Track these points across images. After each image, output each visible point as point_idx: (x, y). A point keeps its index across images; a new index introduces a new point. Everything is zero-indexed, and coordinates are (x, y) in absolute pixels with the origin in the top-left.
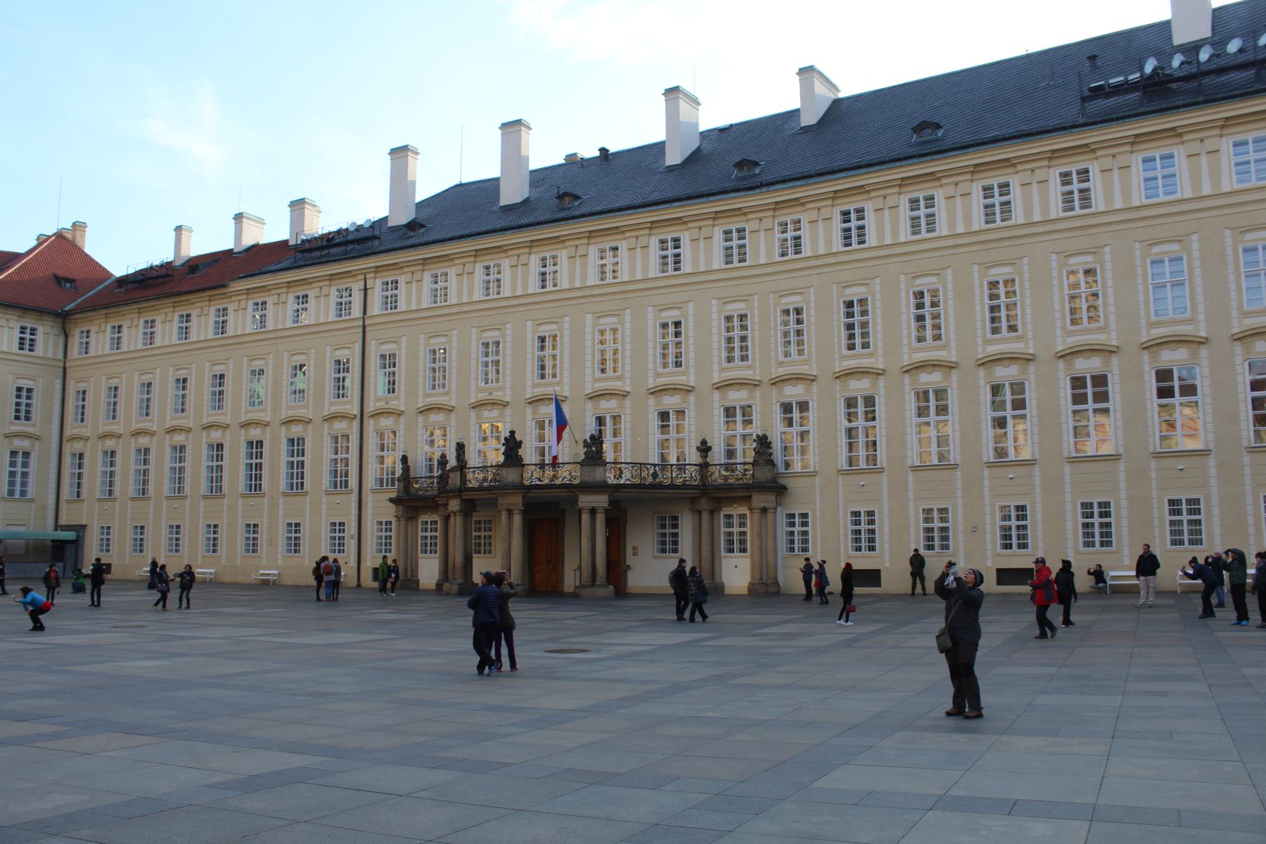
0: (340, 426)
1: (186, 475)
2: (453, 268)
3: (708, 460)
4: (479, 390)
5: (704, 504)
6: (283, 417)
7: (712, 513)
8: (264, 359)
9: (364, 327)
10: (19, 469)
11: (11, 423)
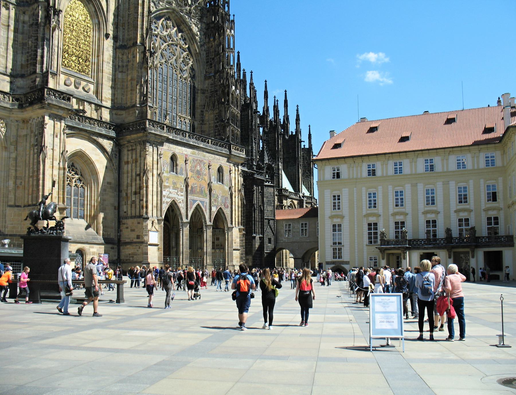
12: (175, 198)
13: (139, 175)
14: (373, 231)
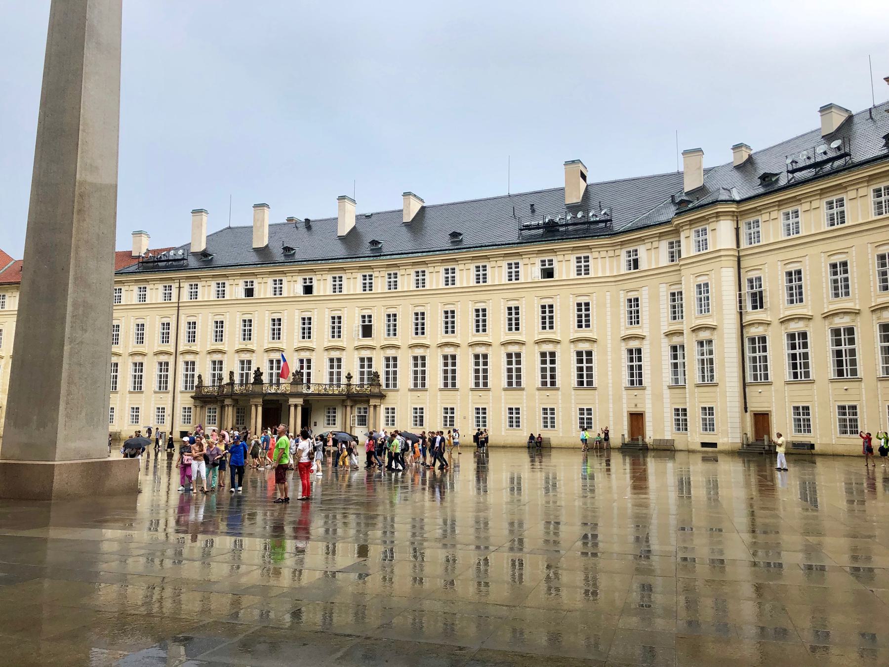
0: (164, 358)
3: (351, 382)
4: (240, 344)
5: (349, 403)
7: (352, 407)
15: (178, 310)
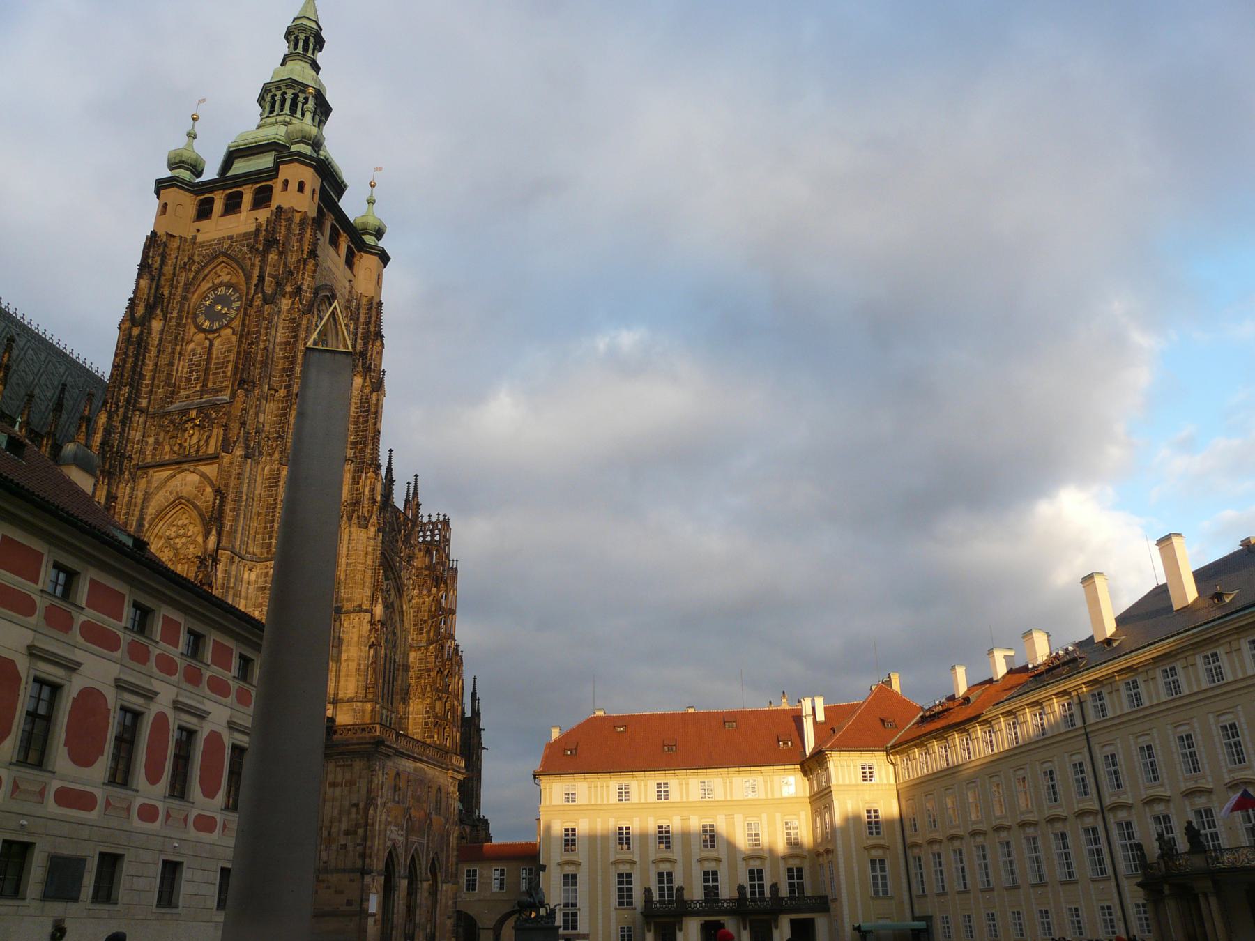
0: (1089, 821)
1: (1072, 860)
2: (1178, 663)
4: (1186, 780)
6: (1047, 816)
8: (1080, 753)
9: (1087, 734)
10: (879, 873)
11: (868, 838)
12: (395, 840)
13: (356, 805)
14: (625, 886)
15: (1088, 739)
